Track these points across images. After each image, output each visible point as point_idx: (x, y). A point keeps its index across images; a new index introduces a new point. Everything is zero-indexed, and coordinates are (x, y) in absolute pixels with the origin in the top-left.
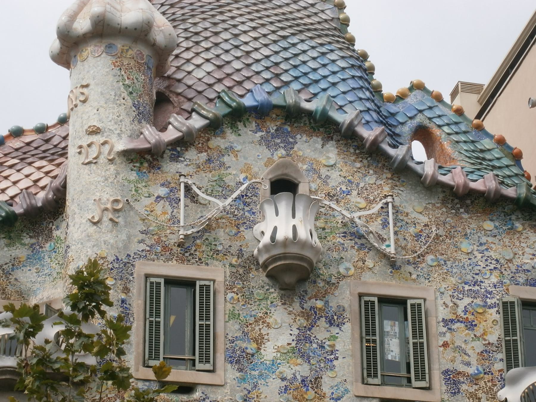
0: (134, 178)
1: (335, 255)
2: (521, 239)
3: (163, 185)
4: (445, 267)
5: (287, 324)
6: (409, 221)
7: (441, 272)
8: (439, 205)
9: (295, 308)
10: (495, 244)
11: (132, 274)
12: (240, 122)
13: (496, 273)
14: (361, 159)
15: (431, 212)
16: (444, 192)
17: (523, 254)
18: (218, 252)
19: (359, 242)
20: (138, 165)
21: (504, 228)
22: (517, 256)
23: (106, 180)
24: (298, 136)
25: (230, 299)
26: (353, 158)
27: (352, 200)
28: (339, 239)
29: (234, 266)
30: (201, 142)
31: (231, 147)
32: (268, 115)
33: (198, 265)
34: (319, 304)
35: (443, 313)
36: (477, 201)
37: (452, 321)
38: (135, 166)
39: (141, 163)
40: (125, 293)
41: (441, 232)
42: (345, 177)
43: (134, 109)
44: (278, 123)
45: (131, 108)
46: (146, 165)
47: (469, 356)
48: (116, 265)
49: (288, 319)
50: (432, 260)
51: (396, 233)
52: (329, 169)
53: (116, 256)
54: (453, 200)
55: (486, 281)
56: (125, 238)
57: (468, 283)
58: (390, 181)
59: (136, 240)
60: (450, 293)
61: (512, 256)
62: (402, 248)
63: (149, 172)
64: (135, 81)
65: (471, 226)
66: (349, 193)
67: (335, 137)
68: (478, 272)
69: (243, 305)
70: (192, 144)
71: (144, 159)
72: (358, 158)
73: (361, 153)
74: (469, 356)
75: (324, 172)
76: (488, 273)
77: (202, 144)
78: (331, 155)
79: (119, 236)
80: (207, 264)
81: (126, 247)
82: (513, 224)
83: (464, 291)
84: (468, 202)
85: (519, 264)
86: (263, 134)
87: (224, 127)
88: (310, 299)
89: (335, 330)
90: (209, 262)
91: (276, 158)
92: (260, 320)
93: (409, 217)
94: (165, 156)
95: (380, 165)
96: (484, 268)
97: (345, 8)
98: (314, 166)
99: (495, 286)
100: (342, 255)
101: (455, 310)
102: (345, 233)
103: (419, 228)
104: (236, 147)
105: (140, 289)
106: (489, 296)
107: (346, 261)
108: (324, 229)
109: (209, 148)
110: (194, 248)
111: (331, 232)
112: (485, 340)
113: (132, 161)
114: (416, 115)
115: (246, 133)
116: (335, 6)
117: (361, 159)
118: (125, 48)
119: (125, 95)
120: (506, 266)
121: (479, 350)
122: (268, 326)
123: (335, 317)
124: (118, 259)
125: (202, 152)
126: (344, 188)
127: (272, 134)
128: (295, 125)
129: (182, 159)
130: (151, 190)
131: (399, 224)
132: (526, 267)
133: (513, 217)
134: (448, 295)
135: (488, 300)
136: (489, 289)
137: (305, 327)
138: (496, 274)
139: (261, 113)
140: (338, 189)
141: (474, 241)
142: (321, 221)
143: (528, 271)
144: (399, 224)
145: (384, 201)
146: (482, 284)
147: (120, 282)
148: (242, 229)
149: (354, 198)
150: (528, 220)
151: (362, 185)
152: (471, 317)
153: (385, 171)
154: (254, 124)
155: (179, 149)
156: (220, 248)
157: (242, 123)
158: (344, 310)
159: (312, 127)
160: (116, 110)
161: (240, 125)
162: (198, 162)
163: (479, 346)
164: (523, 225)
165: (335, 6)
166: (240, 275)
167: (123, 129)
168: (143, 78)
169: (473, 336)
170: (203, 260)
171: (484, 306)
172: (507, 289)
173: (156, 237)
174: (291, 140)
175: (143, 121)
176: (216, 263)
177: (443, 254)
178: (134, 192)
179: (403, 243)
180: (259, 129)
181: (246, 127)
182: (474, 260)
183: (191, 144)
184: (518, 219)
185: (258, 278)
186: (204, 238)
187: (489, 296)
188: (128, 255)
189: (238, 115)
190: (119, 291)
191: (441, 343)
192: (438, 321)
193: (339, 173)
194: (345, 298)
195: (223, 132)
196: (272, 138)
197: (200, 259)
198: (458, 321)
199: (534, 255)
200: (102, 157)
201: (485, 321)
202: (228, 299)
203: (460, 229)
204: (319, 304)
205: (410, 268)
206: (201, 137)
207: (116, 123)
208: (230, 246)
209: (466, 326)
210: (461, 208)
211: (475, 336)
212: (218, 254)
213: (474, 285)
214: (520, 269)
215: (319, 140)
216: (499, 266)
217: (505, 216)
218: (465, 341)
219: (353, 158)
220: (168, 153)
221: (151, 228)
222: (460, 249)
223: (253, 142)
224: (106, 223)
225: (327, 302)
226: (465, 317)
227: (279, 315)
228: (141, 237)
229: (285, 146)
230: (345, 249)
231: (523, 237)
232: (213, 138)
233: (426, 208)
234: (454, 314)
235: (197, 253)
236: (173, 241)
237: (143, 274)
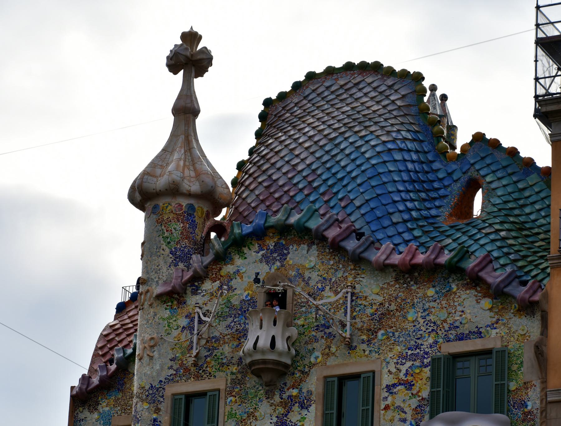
0: (167, 316)
1: (310, 347)
2: (456, 300)
3: (187, 317)
4: (393, 338)
5: (269, 415)
6: (367, 304)
7: (388, 343)
8: (392, 283)
9: (276, 400)
10: (434, 308)
11: (162, 396)
12: (245, 247)
13: (432, 335)
14: (334, 257)
15: (386, 291)
16: (395, 271)
17: (455, 312)
18: (222, 365)
19: (327, 331)
20: (170, 304)
21: (443, 291)
22: (451, 315)
23: (148, 322)
24: (291, 247)
25: (229, 403)
26: (329, 257)
27: (325, 295)
28: (314, 333)
29: (234, 374)
30: (214, 273)
31: (238, 271)
32: (266, 235)
33: (209, 379)
34: (295, 392)
35: (387, 380)
36: (422, 272)
37: (394, 385)
38: (168, 306)
39: (172, 302)
40: (157, 413)
41: (393, 307)
42: (321, 276)
43: (171, 256)
44: (275, 240)
45: (168, 256)
46: (175, 302)
47: (406, 413)
48: (151, 392)
49: (269, 410)
50: (383, 335)
51: (353, 318)
52: (311, 271)
53: (151, 384)
54: (404, 276)
55: (425, 343)
56: (158, 368)
57: (411, 348)
58: (353, 272)
59: (167, 368)
60: (395, 361)
61: (446, 315)
62: (359, 329)
63: (178, 308)
64: (173, 231)
65: (418, 295)
66: (323, 290)
67: (316, 242)
68: (419, 336)
69: (240, 405)
70: (206, 277)
71: (173, 298)
72: (332, 256)
73: (333, 252)
74: (406, 413)
75: (307, 274)
76: (427, 335)
77: (216, 274)
78: (312, 259)
79: (154, 367)
80: (215, 376)
81: (159, 374)
82: (451, 286)
83: (407, 357)
84: (416, 274)
85: (451, 322)
86: (264, 252)
87: (232, 255)
88: (288, 389)
89: (304, 412)
90: (216, 374)
91: (273, 270)
92: (251, 415)
93: (368, 300)
94: (188, 292)
95: (346, 259)
96: (425, 331)
97: (423, 79)
98: (300, 271)
99: (431, 347)
100: (314, 346)
101: (398, 374)
102: (318, 326)
103: (375, 307)
104: (242, 270)
105: (167, 407)
106: (426, 356)
107: (317, 351)
108: (303, 326)
109: (221, 276)
110: (205, 365)
111: (308, 328)
112: (419, 396)
113: (165, 302)
114: (469, 169)
115: (251, 255)
116: (413, 80)
117: (334, 257)
118: (166, 205)
119: (164, 246)
120: (441, 326)
121: (413, 407)
122: (256, 419)
123: (305, 401)
124: (152, 387)
125: (215, 281)
126: (320, 286)
127: (271, 250)
128: (288, 238)
129: (200, 291)
130: (179, 323)
131: (357, 309)
132: (457, 324)
133: (451, 280)
134: (393, 363)
135: (425, 360)
136: (426, 350)
137: (283, 414)
138: (433, 336)
139: (259, 235)
140: (316, 287)
141: (419, 308)
142: (302, 319)
143: (457, 327)
144: (357, 309)
145: (344, 290)
146: (422, 347)
147: (152, 405)
148: (242, 340)
149: (327, 292)
150: (460, 280)
151: (333, 280)
152: (410, 378)
153: (350, 263)
154: (257, 245)
155: (196, 284)
156: (224, 361)
157: (247, 247)
158: (311, 394)
159: (300, 237)
160: (157, 261)
161: (246, 250)
162: (212, 291)
163: (414, 403)
164: (457, 285)
165: (413, 80)
166: (239, 380)
167: (160, 277)
168: (182, 225)
169: (410, 395)
170: (212, 373)
171: (421, 367)
172: (440, 348)
173: (180, 362)
174: (285, 252)
175: (180, 264)
176: (221, 374)
177: (392, 327)
178: (167, 328)
179: (359, 325)
180: (261, 249)
181: (250, 249)
182: (418, 327)
183: (205, 277)
184: (454, 281)
185: (251, 381)
186: (214, 354)
187: (426, 356)
188: (161, 381)
189: (239, 244)
190: (152, 412)
191: (383, 407)
192: (382, 387)
193: (317, 273)
194: (313, 384)
195: (232, 259)
196: (271, 254)
197: (210, 373)
198: (400, 384)
199: (463, 312)
200: (146, 303)
201: (421, 379)
202: (228, 403)
203: (409, 301)
204: (295, 392)
205: (364, 346)
206: (213, 269)
207: (156, 272)
208: (232, 357)
209: (406, 387)
210: (411, 281)
211: (412, 394)
212: (223, 366)
213: (416, 349)
214: (452, 326)
215: (306, 247)
216: (435, 328)
217: (444, 280)
218: (404, 400)
219: (329, 257)
220: (189, 290)
221: (177, 355)
222: (407, 319)
223: (256, 262)
224: (146, 359)
225: (300, 390)
226: (406, 379)
227: (264, 408)
228: (170, 363)
229: (280, 258)
230: (317, 340)
231: (456, 297)
232: (224, 266)
233: (382, 289)
234: (396, 379)
235: (208, 369)
236: (190, 363)
237: (170, 394)
